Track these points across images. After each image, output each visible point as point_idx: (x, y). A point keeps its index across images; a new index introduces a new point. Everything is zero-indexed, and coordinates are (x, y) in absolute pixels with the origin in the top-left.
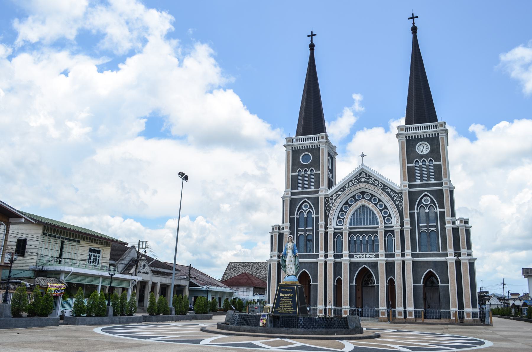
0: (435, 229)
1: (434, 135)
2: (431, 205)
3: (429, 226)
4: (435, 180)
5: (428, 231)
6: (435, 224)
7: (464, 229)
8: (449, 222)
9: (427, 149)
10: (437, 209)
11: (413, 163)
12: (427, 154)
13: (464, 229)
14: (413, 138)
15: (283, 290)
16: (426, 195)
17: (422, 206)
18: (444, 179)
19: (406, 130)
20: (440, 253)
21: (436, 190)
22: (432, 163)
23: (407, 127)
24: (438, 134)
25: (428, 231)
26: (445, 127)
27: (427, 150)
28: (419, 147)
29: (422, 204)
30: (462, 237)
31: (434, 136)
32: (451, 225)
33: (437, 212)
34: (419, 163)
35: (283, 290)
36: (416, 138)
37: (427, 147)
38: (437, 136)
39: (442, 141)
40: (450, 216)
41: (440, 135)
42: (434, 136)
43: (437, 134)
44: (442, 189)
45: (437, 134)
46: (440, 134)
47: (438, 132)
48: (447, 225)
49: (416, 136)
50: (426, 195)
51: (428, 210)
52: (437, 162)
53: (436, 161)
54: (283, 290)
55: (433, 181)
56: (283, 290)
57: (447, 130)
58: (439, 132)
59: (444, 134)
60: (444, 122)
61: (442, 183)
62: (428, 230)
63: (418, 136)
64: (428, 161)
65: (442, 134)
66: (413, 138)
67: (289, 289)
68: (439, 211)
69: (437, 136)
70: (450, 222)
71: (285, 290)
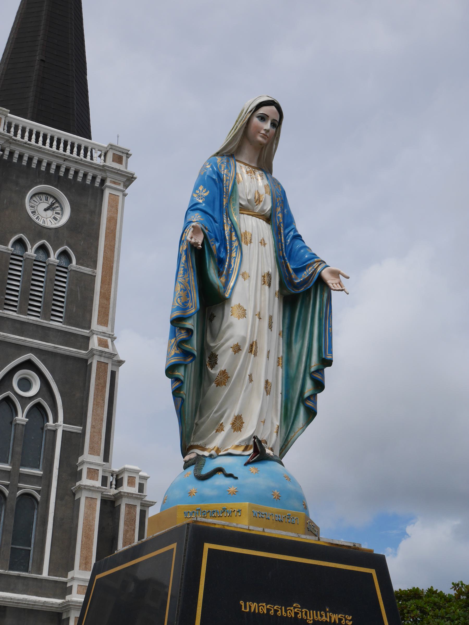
0: (36, 491)
1: (89, 177)
2: (39, 406)
3: (20, 473)
4: (68, 321)
5: (13, 493)
6: (39, 472)
7: (135, 506)
8: (92, 474)
9: (58, 216)
10: (55, 420)
11: (6, 245)
12: (56, 229)
13: (135, 506)
14: (24, 163)
15: (253, 606)
16: (29, 364)
17: (8, 400)
18: (95, 325)
19: (6, 128)
20: (42, 580)
21: (66, 357)
22: (64, 265)
23: (11, 120)
24: (103, 181)
25: (13, 493)
26: (126, 168)
27: (55, 219)
28: (34, 199)
29: (9, 393)
30: (126, 532)
31: (88, 182)
32: (98, 483)
33: (55, 432)
34: (25, 248)
35: (263, 608)
36: (34, 166)
37: (59, 208)
38: (97, 185)
39: (112, 207)
40: (99, 455)
41: (108, 183)
42: (88, 182)
43: (98, 180)
44: (85, 357)
45: (98, 180)
46: (111, 182)
47: (104, 175)
48: (85, 481)
49: (35, 161)
50: (29, 364)
51: (26, 418)
52: (82, 265)
53: (81, 261)
54: (263, 608)
55: (57, 324)
56: (253, 606)
57: (133, 177)
58: (108, 174)
59: (121, 187)
60: (127, 154)
61: (88, 339)
62: (13, 487)
63: (40, 162)
64: (56, 256)
65: (115, 183)
66: (24, 163)
67: (319, 607)
68: (64, 431)
69: (97, 185)
70: (98, 474)
71: (282, 612)
